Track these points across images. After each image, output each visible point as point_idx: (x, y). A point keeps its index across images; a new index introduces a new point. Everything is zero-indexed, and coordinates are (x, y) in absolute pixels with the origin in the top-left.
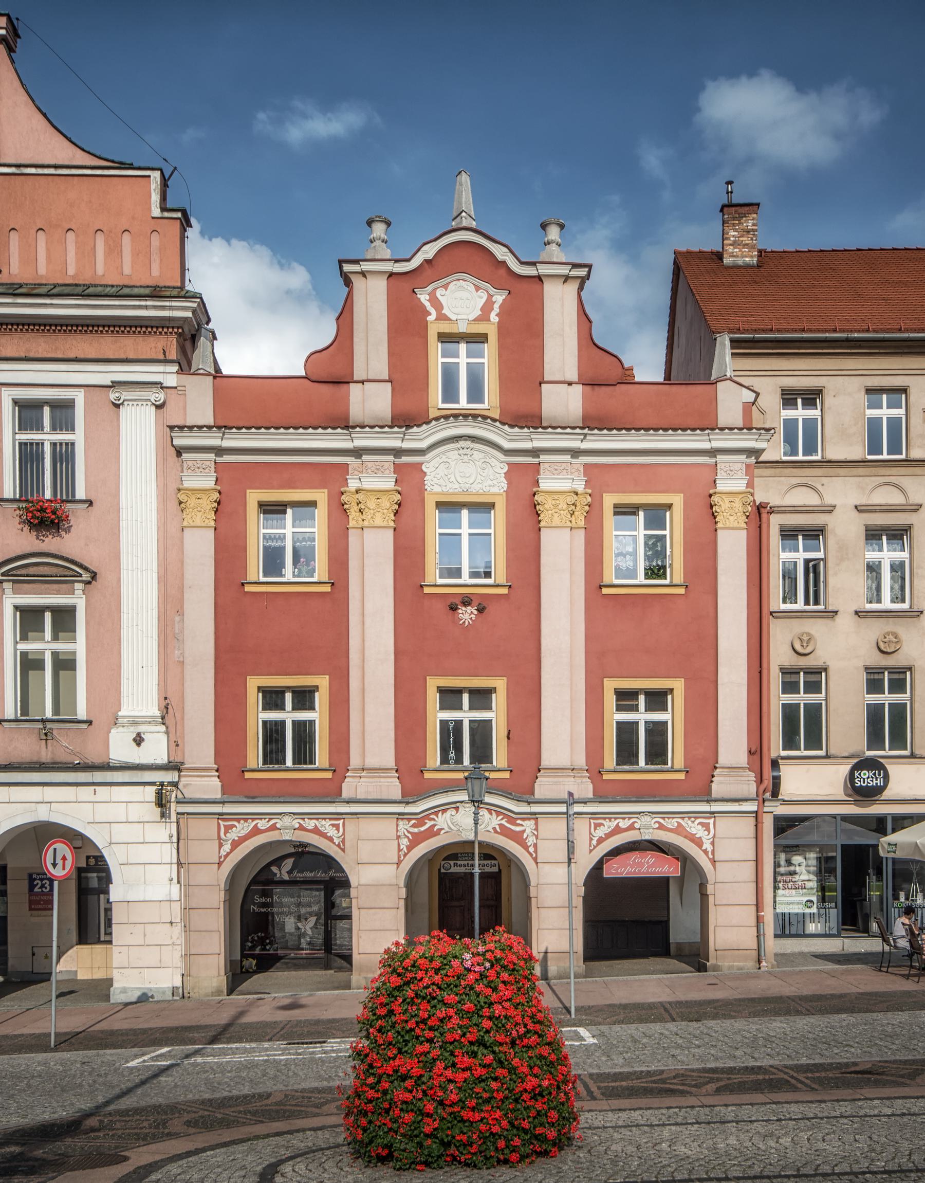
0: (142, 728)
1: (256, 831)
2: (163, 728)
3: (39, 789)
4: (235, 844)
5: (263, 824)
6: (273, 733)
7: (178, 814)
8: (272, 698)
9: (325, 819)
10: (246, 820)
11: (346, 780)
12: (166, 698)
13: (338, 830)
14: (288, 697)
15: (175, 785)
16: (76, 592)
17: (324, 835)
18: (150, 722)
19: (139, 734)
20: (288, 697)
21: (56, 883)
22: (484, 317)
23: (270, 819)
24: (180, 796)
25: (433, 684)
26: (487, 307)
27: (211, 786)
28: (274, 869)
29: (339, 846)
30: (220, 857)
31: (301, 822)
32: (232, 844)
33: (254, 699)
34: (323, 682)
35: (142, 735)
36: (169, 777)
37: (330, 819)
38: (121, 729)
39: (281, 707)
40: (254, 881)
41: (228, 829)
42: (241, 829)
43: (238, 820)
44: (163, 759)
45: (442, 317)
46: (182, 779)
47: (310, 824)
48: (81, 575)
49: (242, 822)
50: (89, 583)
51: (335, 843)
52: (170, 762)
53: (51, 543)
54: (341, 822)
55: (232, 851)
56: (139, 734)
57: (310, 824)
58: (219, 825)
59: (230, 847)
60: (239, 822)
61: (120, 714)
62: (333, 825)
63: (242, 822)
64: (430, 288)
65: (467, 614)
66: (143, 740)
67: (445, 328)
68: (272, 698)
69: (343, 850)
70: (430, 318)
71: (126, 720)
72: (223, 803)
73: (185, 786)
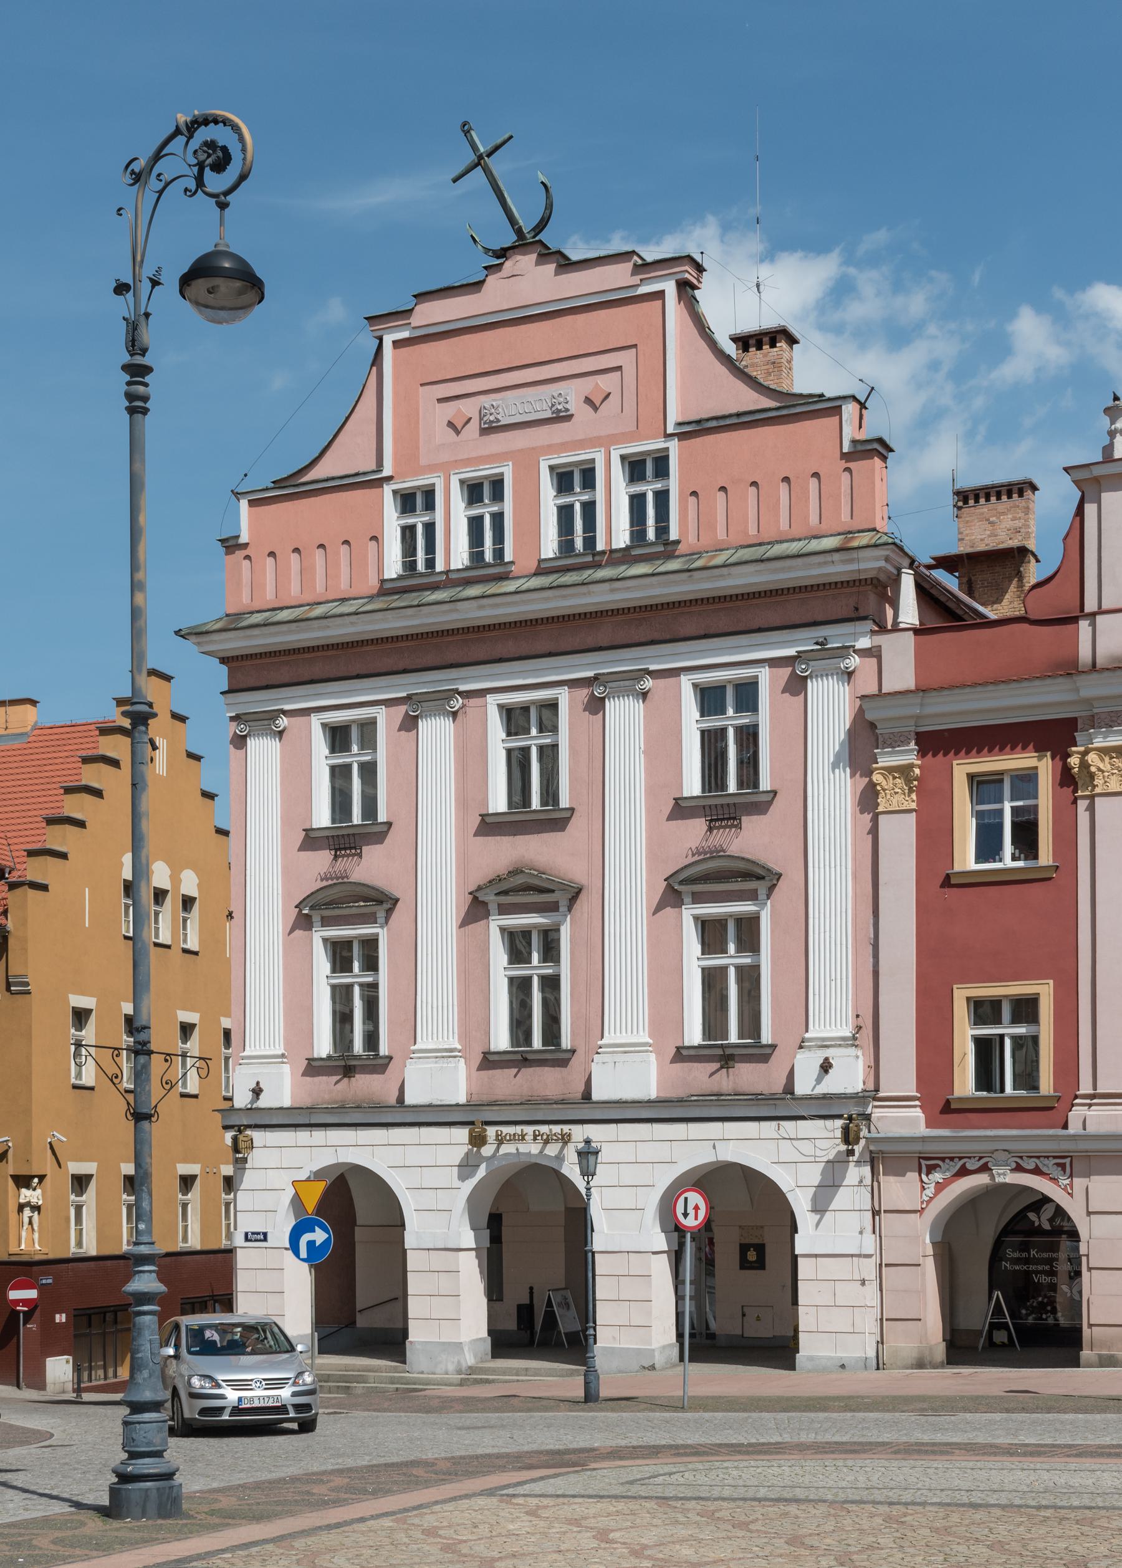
0: (829, 1053)
3: (719, 1125)
9: (1048, 1157)
10: (952, 1159)
11: (1074, 1108)
12: (858, 1016)
13: (1064, 1170)
18: (840, 1045)
19: (826, 1059)
21: (688, 1235)
23: (981, 1158)
28: (1032, 1216)
29: (1065, 1189)
30: (922, 1203)
31: (1019, 1160)
32: (935, 1188)
33: (961, 1012)
35: (831, 1061)
37: (1055, 1157)
39: (997, 1021)
40: (1007, 1231)
43: (943, 1159)
49: (947, 1161)
51: (1060, 1186)
54: (1068, 1161)
55: (936, 1194)
56: (826, 1059)
59: (933, 1190)
62: (1058, 1165)
63: (947, 1161)
66: (831, 1066)
69: (1071, 1195)
73: (879, 1118)
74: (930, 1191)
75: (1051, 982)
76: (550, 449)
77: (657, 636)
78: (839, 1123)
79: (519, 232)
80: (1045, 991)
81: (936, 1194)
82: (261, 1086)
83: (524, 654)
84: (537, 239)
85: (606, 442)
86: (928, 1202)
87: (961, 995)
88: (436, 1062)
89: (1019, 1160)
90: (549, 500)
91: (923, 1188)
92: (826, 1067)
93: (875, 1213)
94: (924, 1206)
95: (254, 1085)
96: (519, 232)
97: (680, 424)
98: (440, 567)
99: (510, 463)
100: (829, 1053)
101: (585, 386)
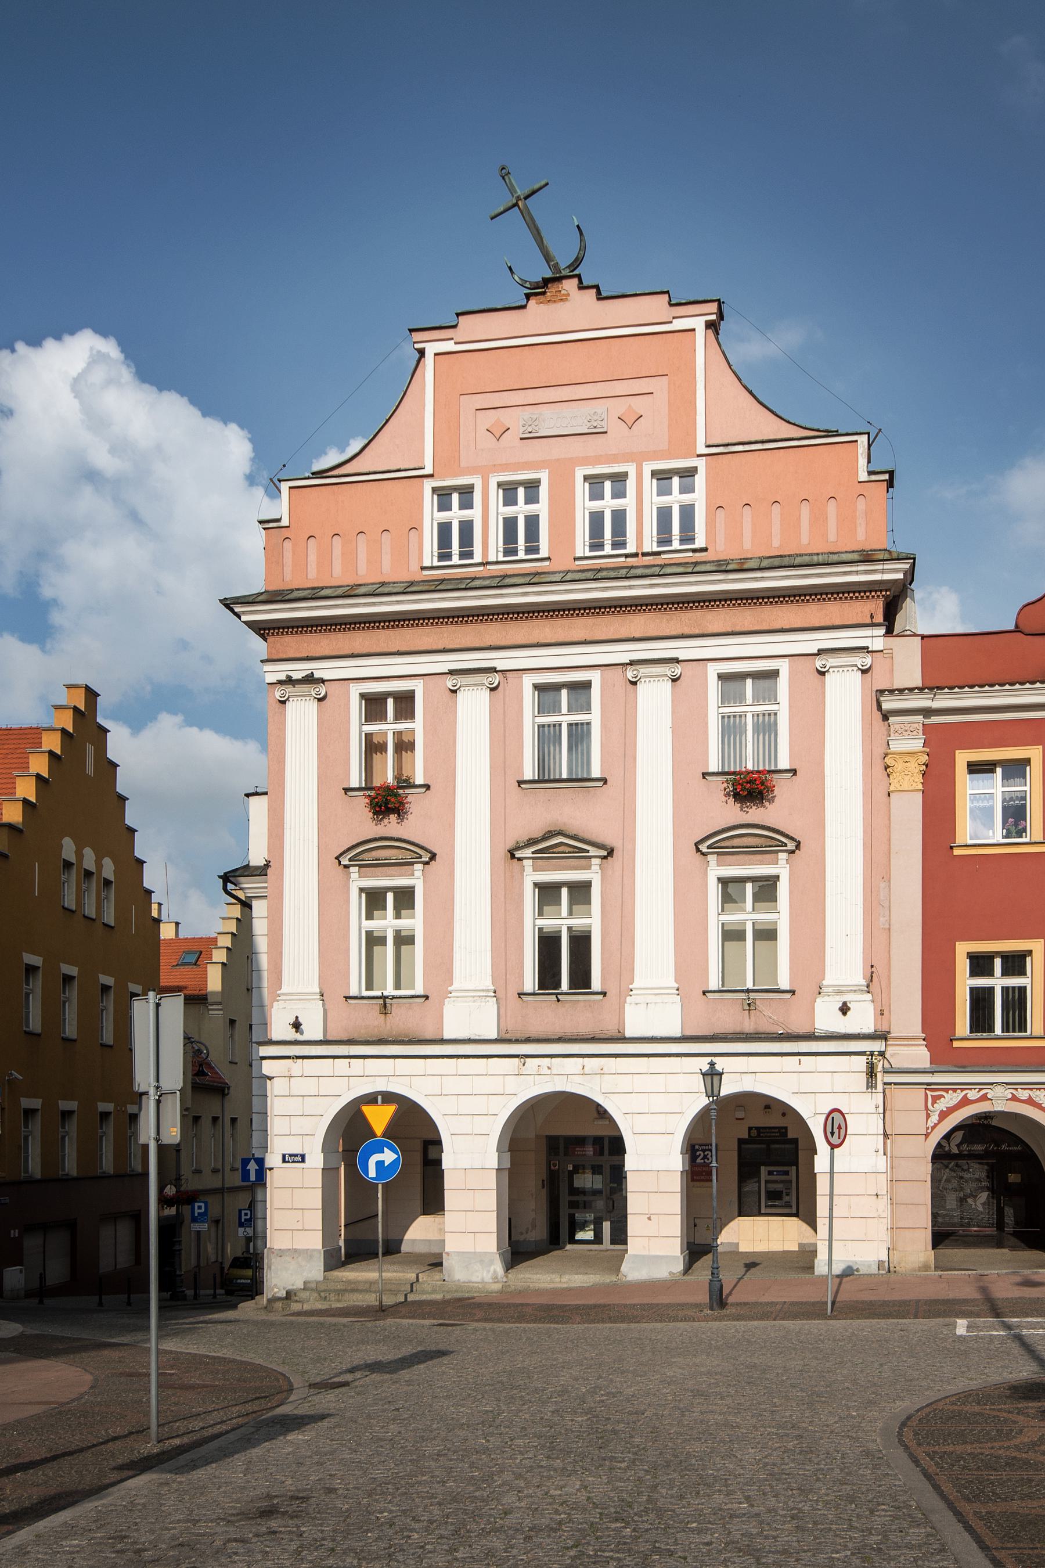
0: (846, 997)
1: (965, 1102)
2: (869, 997)
4: (943, 1115)
5: (973, 1095)
6: (981, 1000)
7: (885, 1084)
8: (980, 964)
9: (1039, 1089)
10: (955, 1090)
12: (872, 966)
14: (998, 962)
15: (882, 1054)
16: (780, 862)
18: (855, 991)
19: (845, 1004)
20: (998, 962)
23: (981, 1089)
24: (887, 1065)
27: (919, 1055)
30: (928, 1128)
31: (1014, 1092)
33: (963, 965)
35: (848, 1004)
36: (877, 1046)
38: (826, 998)
39: (990, 973)
41: (935, 1099)
42: (951, 1099)
43: (947, 1091)
44: (869, 1028)
46: (889, 1048)
47: (1024, 1095)
48: (786, 845)
49: (950, 1092)
50: (793, 852)
52: (875, 1031)
53: (755, 814)
55: (940, 1121)
56: (845, 1004)
57: (1024, 1095)
58: (926, 1095)
60: (948, 1093)
61: (825, 983)
63: (950, 1092)
66: (849, 1009)
68: (980, 964)
71: (831, 989)
72: (933, 1072)
73: (892, 1056)
74: (934, 1118)
75: (1042, 940)
76: (585, 461)
77: (687, 631)
78: (863, 1060)
81: (940, 1121)
82: (300, 1019)
83: (561, 640)
84: (574, 273)
85: (638, 459)
86: (933, 1128)
87: (963, 949)
88: (474, 1001)
89: (1014, 1092)
91: (928, 1116)
93: (886, 1135)
94: (929, 1131)
95: (292, 1020)
98: (478, 558)
99: (547, 471)
101: (620, 407)
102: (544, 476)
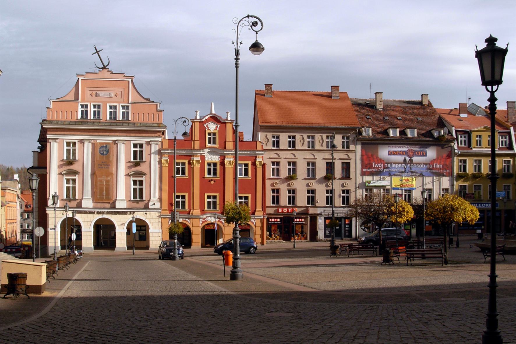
0: (155, 202)
17: (187, 221)
22: (216, 129)
25: (206, 195)
26: (217, 128)
34: (186, 194)
45: (208, 129)
47: (184, 219)
64: (206, 124)
65: (212, 182)
67: (209, 131)
70: (206, 129)
76: (109, 102)
79: (104, 65)
80: (186, 194)
85: (119, 103)
90: (109, 110)
92: (154, 204)
96: (104, 65)
97: (131, 102)
100: (155, 202)
102: (101, 104)
